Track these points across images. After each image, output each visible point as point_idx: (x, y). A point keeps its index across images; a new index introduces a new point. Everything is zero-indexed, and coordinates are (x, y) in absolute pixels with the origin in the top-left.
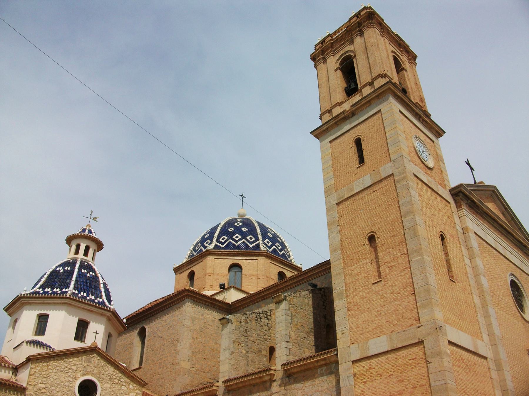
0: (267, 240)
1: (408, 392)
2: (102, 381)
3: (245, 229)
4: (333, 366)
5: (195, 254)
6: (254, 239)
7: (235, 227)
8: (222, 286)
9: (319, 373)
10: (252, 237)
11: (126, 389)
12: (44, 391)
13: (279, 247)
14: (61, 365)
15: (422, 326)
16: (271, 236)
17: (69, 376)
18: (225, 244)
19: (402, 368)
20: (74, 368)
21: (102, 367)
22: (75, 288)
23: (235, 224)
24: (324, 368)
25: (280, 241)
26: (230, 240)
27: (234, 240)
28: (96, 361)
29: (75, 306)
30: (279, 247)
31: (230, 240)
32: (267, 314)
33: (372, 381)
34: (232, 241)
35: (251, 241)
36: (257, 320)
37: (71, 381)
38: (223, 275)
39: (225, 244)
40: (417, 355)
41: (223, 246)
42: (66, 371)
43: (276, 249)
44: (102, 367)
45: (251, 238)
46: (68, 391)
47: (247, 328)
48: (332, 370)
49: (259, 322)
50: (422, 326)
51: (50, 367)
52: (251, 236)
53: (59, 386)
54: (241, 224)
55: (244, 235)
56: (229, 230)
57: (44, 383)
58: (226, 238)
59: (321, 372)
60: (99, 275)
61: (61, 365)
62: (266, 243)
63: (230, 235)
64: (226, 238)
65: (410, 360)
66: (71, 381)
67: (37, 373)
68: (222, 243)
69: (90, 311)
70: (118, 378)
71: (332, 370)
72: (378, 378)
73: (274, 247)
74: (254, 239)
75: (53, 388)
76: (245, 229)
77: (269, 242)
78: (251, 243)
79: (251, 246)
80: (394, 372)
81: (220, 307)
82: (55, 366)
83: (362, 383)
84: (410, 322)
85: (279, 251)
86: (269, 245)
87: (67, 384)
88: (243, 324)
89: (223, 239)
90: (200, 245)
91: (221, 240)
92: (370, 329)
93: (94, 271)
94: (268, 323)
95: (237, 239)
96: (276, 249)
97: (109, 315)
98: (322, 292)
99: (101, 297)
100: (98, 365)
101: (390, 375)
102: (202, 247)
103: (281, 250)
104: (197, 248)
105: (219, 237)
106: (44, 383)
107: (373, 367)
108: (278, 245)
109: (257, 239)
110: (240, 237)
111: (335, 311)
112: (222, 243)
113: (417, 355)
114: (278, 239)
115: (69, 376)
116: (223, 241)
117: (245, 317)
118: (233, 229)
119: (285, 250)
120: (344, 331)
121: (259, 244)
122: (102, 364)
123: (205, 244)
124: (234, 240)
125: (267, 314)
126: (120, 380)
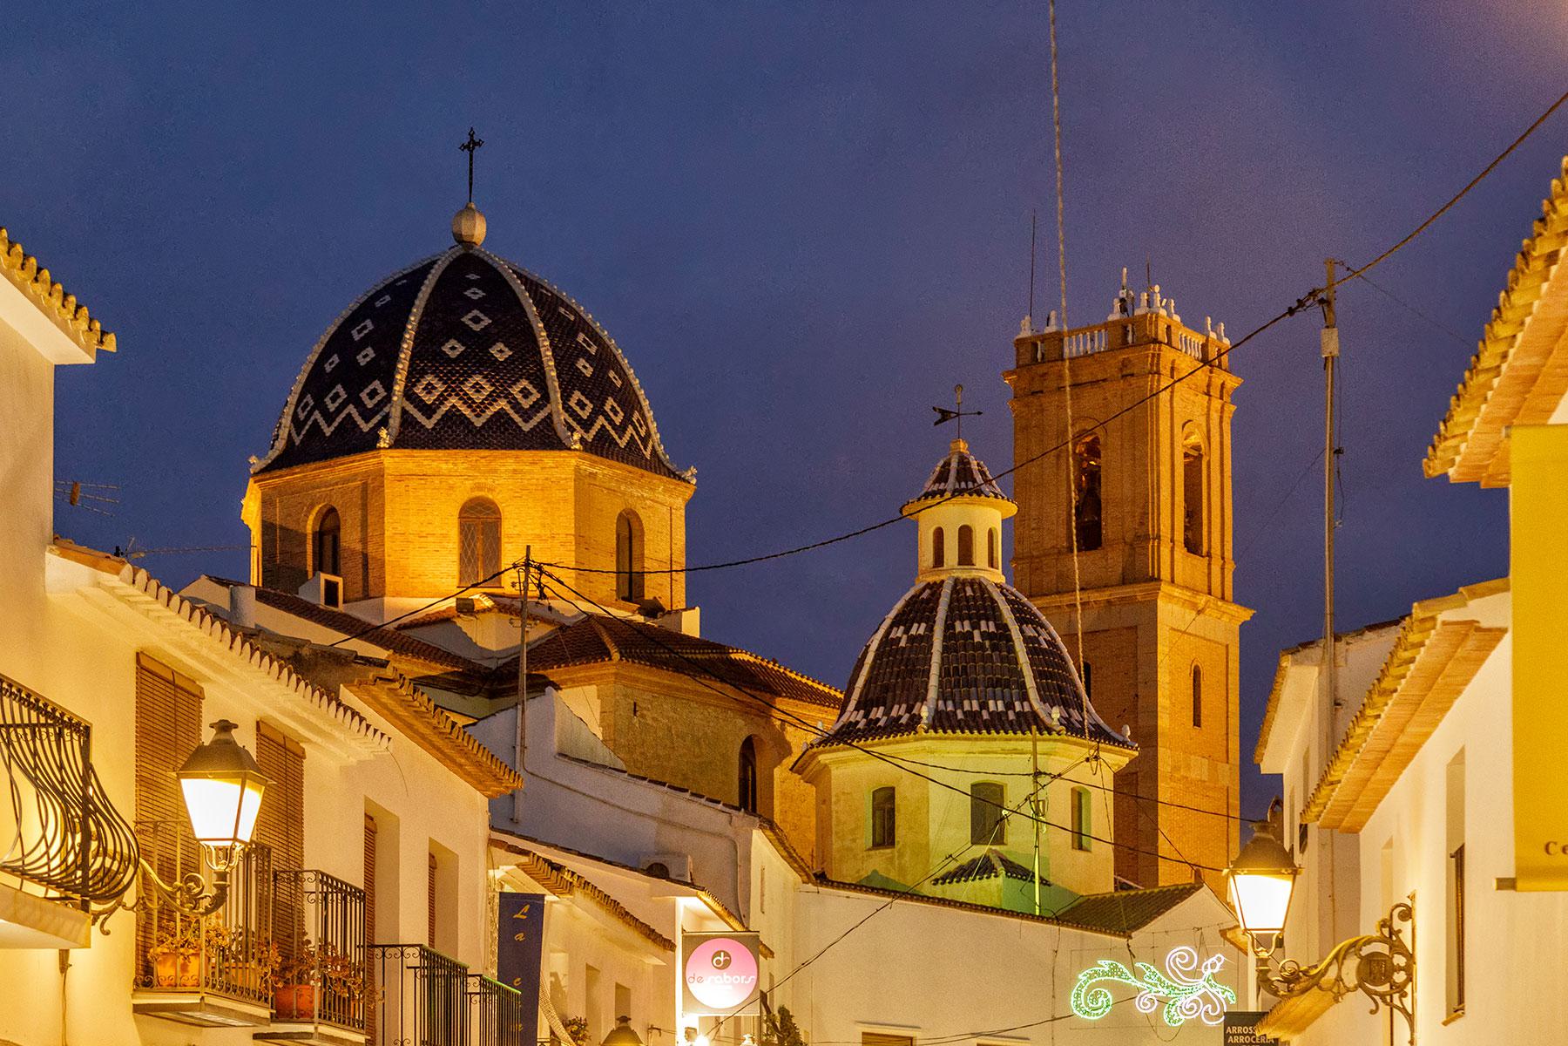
0: (577, 395)
3: (500, 352)
5: (328, 431)
6: (536, 396)
10: (530, 387)
13: (616, 413)
18: (437, 417)
25: (619, 383)
26: (453, 400)
27: (468, 402)
30: (616, 413)
31: (453, 400)
35: (526, 404)
39: (437, 417)
43: (609, 428)
45: (525, 393)
52: (524, 383)
54: (487, 321)
56: (446, 348)
62: (577, 409)
64: (440, 387)
68: (428, 411)
73: (601, 420)
74: (536, 396)
77: (587, 402)
79: (526, 428)
85: (616, 437)
86: (584, 415)
89: (429, 389)
91: (419, 390)
95: (478, 398)
96: (609, 428)
102: (351, 409)
103: (621, 430)
104: (332, 407)
105: (414, 375)
109: (546, 398)
110: (488, 388)
112: (428, 411)
121: (550, 415)
123: (364, 395)
124: (468, 402)
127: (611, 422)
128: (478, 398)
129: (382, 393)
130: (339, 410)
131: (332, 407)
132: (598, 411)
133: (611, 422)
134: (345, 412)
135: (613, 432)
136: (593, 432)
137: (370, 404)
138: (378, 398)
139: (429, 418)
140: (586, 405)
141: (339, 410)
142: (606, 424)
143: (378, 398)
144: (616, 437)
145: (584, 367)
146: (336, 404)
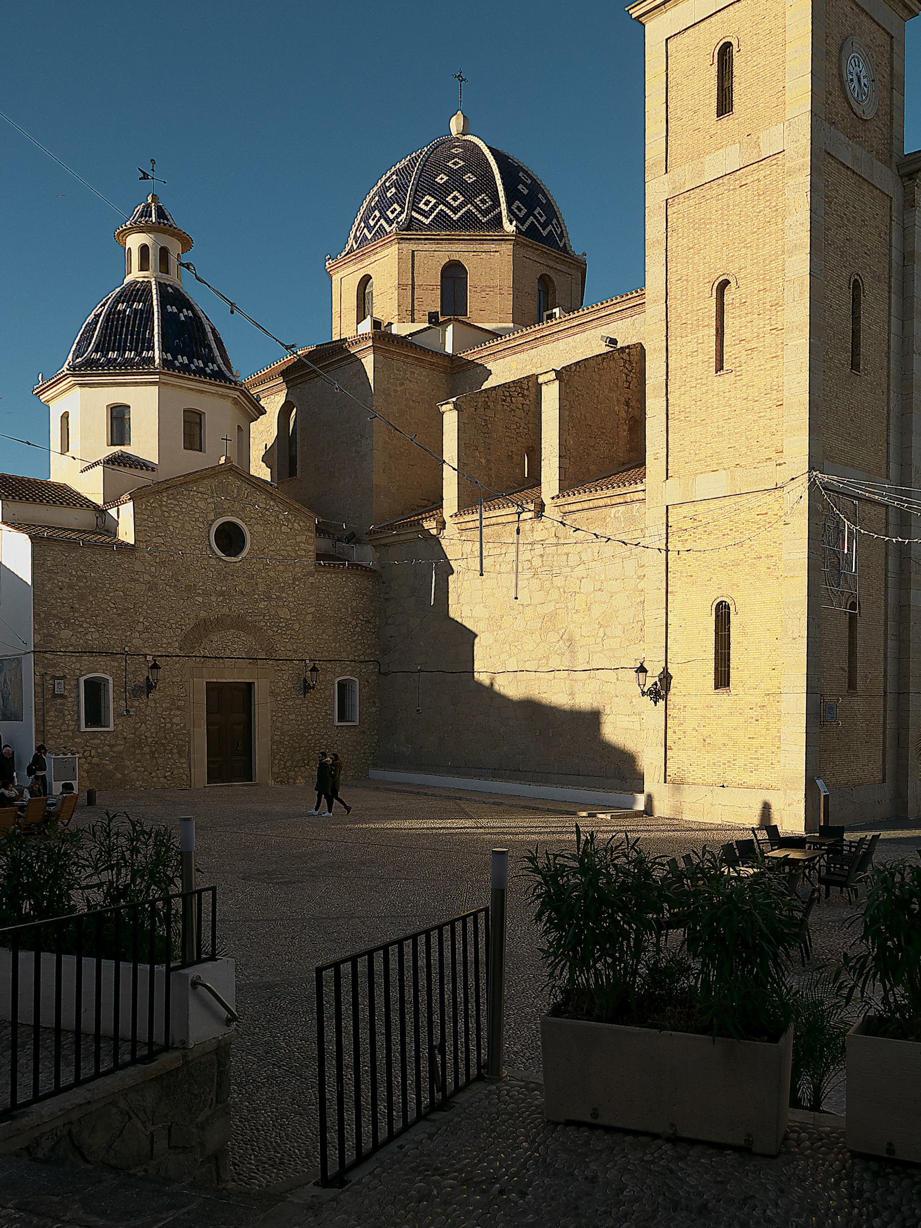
1: (747, 563)
2: (249, 521)
3: (470, 178)
4: (637, 508)
5: (369, 236)
7: (450, 173)
8: (433, 320)
9: (612, 516)
11: (289, 530)
12: (163, 548)
13: (541, 216)
14: (181, 503)
15: (785, 463)
16: (526, 192)
17: (197, 520)
19: (743, 526)
20: (201, 504)
21: (246, 498)
22: (164, 349)
23: (450, 164)
24: (622, 508)
26: (441, 207)
28: (235, 490)
29: (173, 385)
31: (441, 207)
32: (521, 388)
33: (695, 541)
34: (446, 209)
36: (504, 401)
37: (201, 528)
38: (431, 288)
39: (431, 217)
40: (769, 509)
41: (427, 222)
42: (191, 511)
44: (246, 498)
45: (483, 201)
46: (199, 544)
47: (487, 418)
48: (634, 513)
49: (508, 405)
50: (785, 463)
51: (164, 509)
53: (185, 538)
55: (470, 193)
57: (160, 536)
58: (433, 201)
59: (617, 515)
60: (202, 315)
61: (181, 503)
63: (441, 193)
64: (433, 201)
65: (758, 515)
66: (201, 528)
67: (145, 520)
69: (202, 392)
70: (274, 514)
71: (634, 513)
72: (706, 536)
75: (177, 542)
76: (470, 178)
77: (523, 207)
78: (485, 213)
80: (731, 530)
81: (432, 364)
82: (172, 506)
83: (679, 541)
84: (768, 455)
85: (541, 229)
87: (196, 532)
88: (481, 411)
90: (377, 213)
91: (421, 205)
92: (702, 456)
93: (190, 307)
94: (523, 404)
95: (455, 204)
96: (536, 223)
97: (236, 397)
98: (625, 356)
99: (214, 361)
100: (238, 495)
101: (723, 535)
102: (382, 221)
104: (372, 223)
106: (160, 536)
107: (700, 519)
108: (539, 213)
111: (647, 417)
112: (426, 215)
113: (769, 509)
114: (540, 196)
115: (197, 520)
116: (427, 209)
117: (485, 398)
118: (446, 178)
119: (554, 221)
120: (658, 455)
121: (501, 212)
122: (246, 494)
123: (388, 213)
125: (521, 388)
126: (278, 518)
127: (538, 221)
128: (455, 204)
129: (399, 209)
130: (376, 223)
131: (372, 223)
132: (530, 213)
133: (538, 221)
134: (379, 224)
135: (538, 226)
136: (526, 225)
137: (391, 216)
138: (396, 213)
139: (427, 218)
140: (522, 209)
141: (376, 223)
142: (535, 221)
143: (396, 213)
144: (541, 229)
145: (523, 189)
146: (375, 221)
